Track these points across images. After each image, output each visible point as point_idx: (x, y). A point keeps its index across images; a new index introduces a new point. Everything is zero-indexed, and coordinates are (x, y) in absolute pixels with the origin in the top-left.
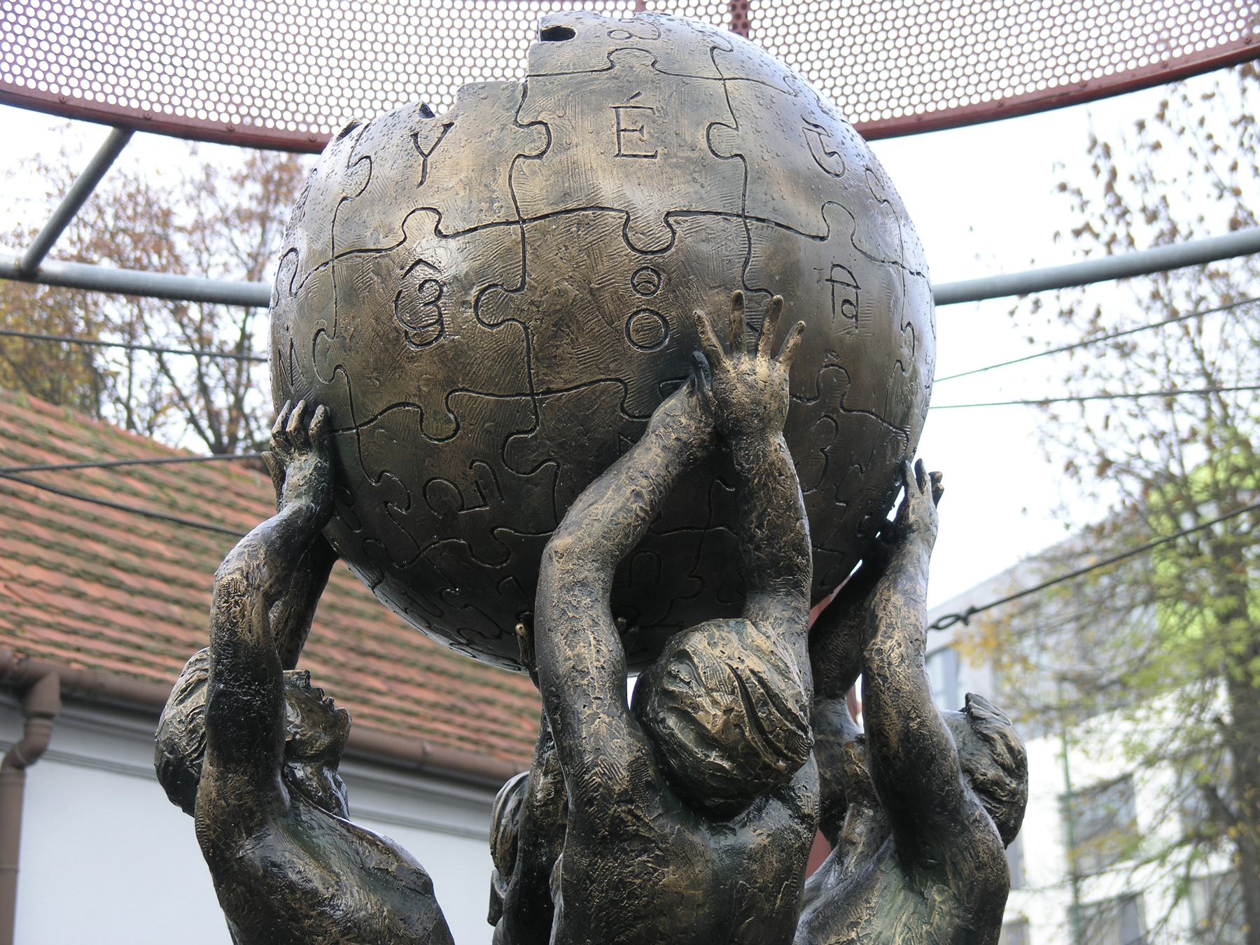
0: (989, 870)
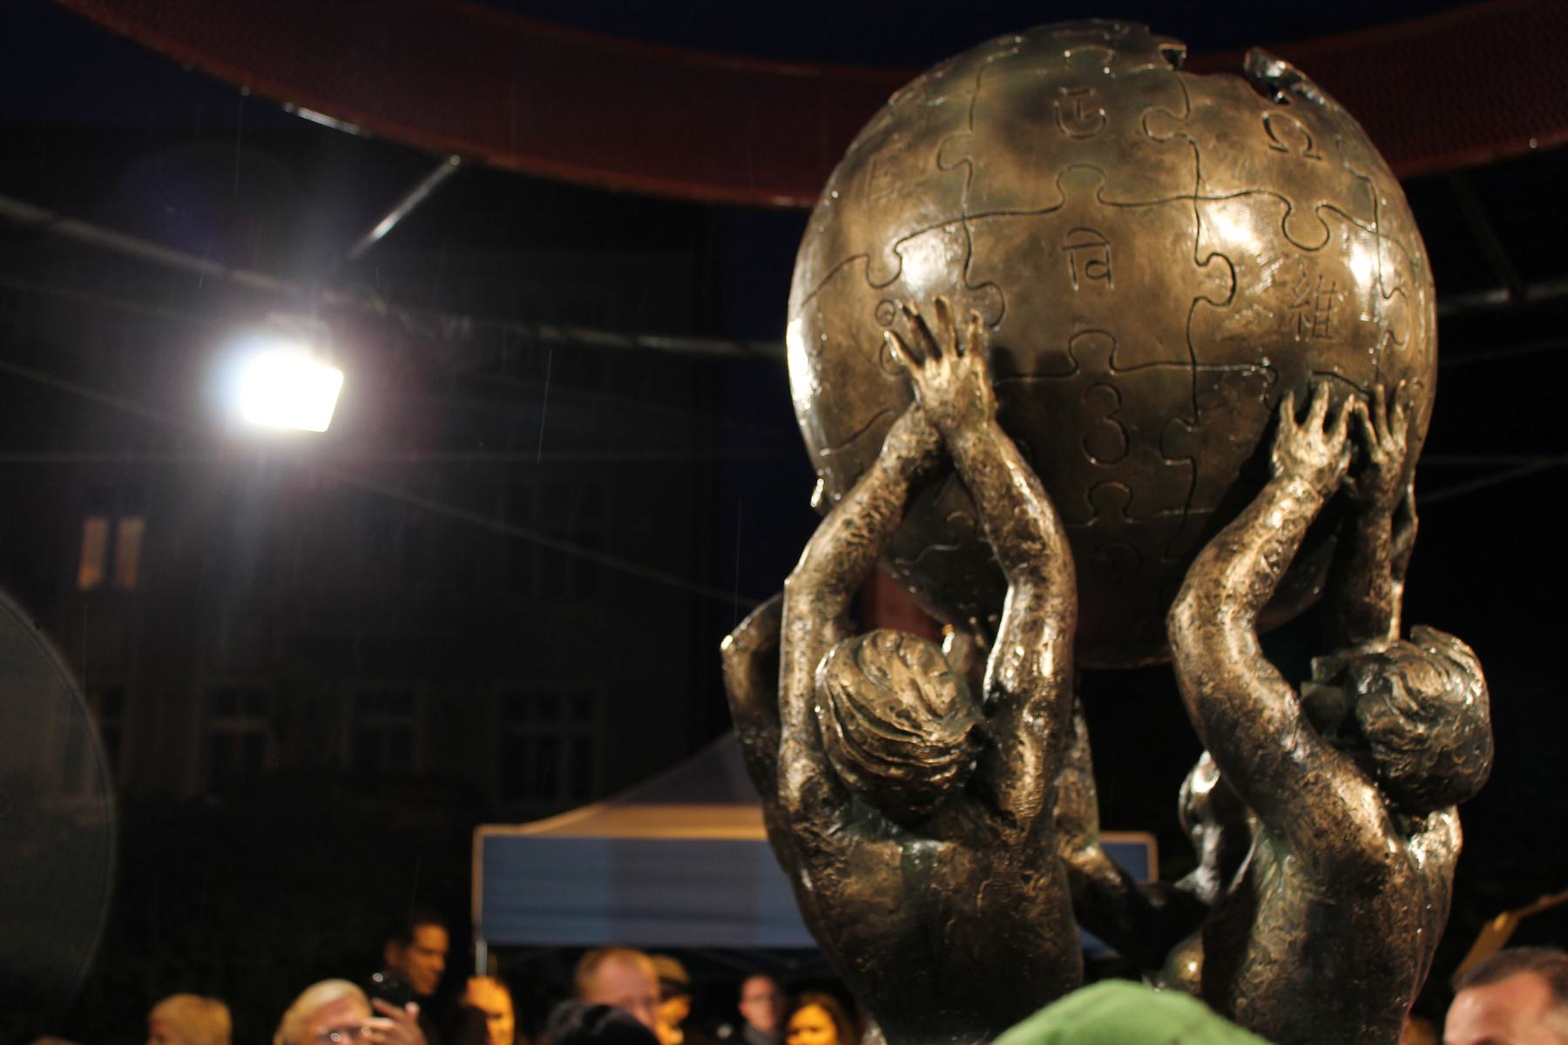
0: (1331, 837)
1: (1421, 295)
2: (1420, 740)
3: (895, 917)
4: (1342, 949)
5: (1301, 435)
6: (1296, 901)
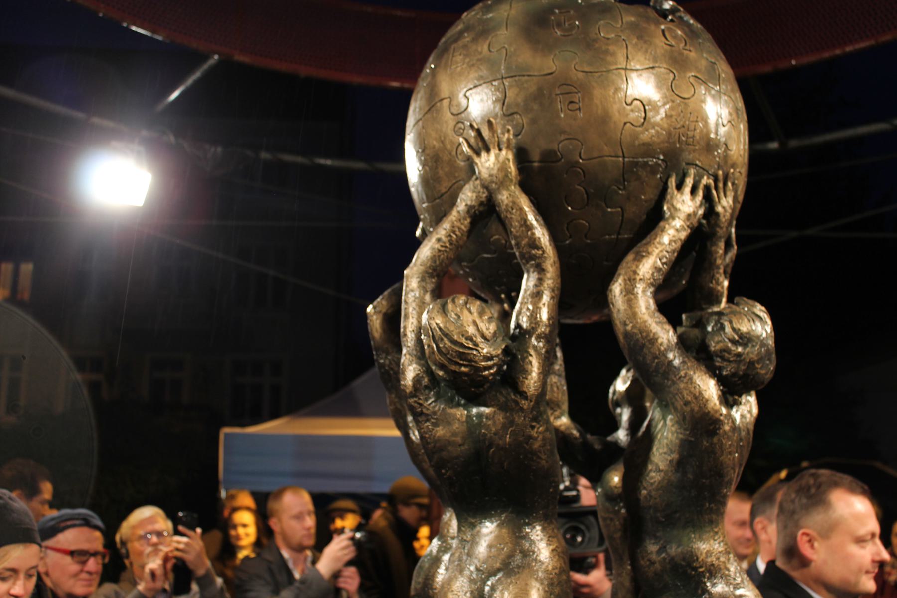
0: (693, 405)
1: (741, 126)
2: (739, 355)
3: (463, 448)
4: (697, 464)
5: (679, 196)
6: (674, 439)
